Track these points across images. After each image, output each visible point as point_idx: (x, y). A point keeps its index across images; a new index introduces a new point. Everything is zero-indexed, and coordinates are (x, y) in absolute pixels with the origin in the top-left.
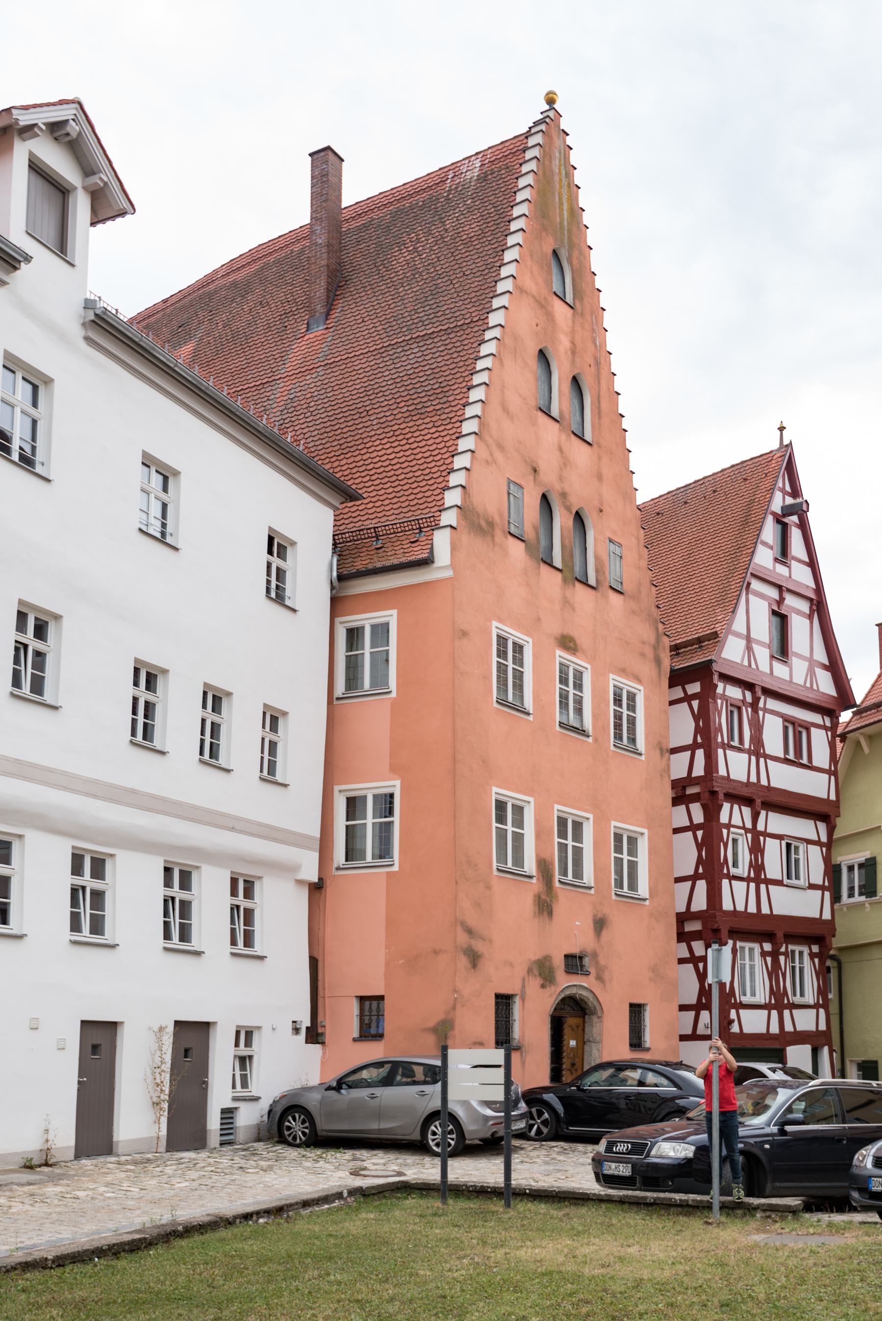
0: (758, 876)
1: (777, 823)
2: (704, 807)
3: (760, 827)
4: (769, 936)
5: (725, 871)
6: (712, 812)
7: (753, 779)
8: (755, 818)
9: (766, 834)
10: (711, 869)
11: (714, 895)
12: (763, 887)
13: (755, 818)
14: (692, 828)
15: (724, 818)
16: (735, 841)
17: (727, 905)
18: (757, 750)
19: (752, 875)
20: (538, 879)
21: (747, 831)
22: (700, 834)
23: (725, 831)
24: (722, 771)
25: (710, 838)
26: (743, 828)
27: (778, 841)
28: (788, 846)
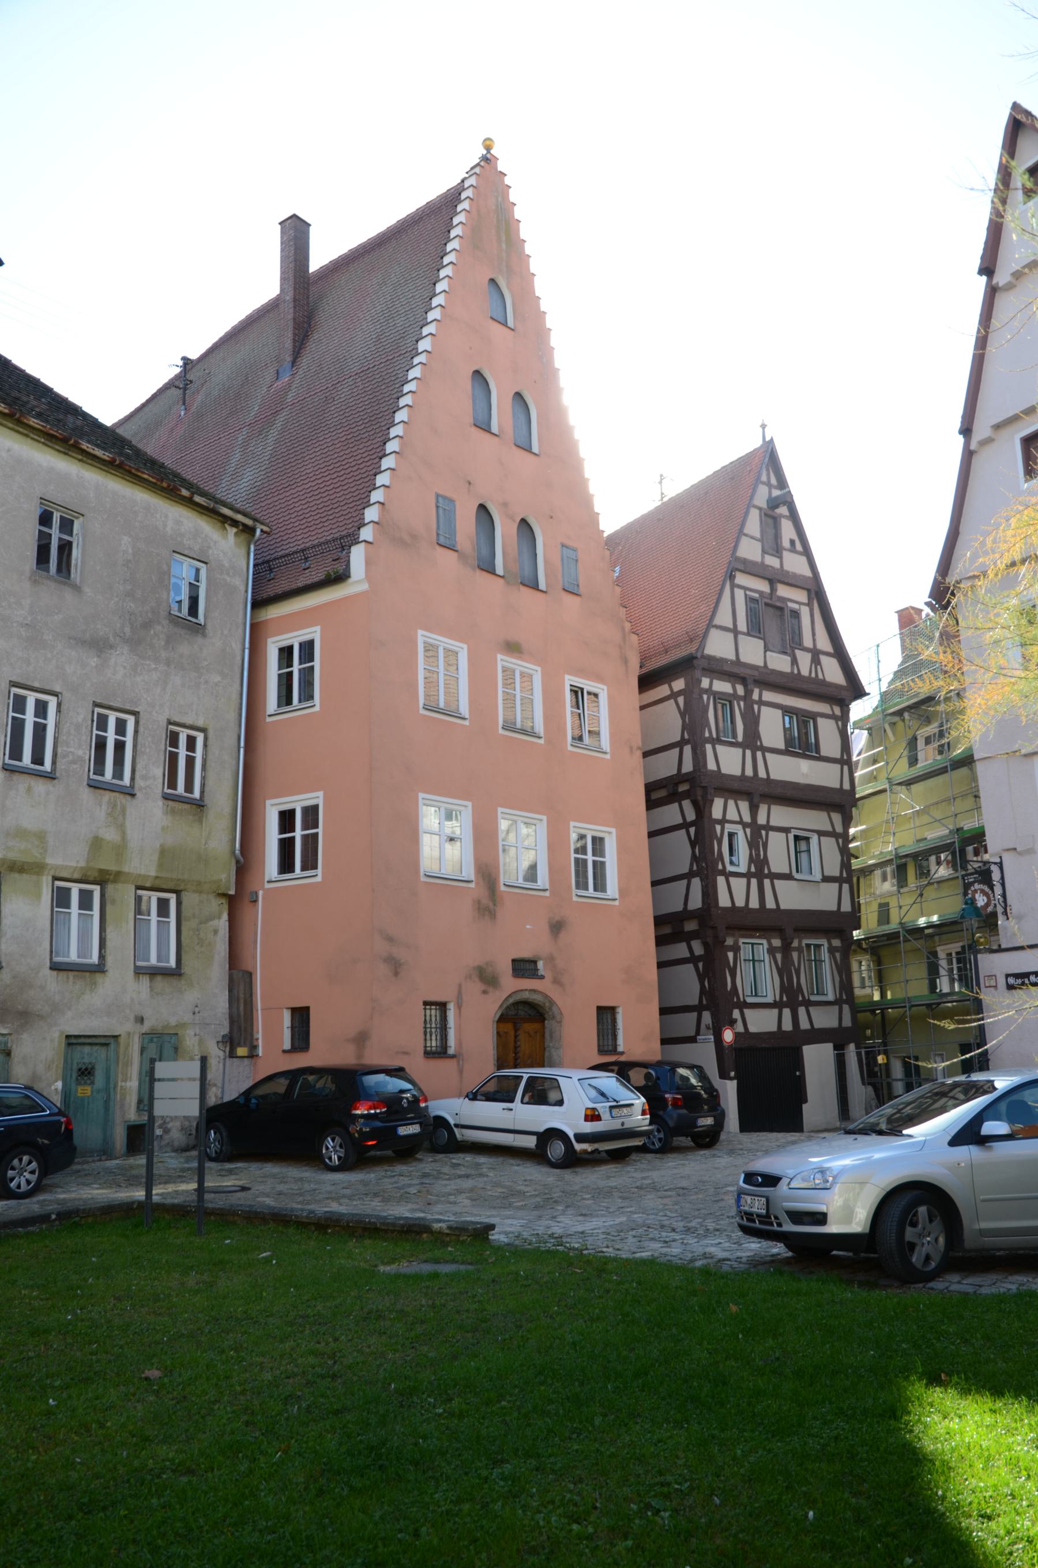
0: (759, 870)
1: (781, 815)
2: (695, 804)
3: (762, 820)
4: (779, 931)
5: (720, 867)
6: (702, 809)
7: (749, 772)
8: (754, 810)
9: (768, 828)
10: (706, 866)
11: (709, 893)
12: (767, 882)
13: (754, 810)
14: (685, 825)
15: (717, 812)
16: (731, 835)
17: (724, 901)
18: (752, 742)
19: (753, 869)
20: (477, 884)
21: (745, 825)
22: (692, 830)
23: (718, 828)
24: (711, 766)
25: (702, 833)
26: (741, 822)
27: (784, 835)
28: (797, 838)
